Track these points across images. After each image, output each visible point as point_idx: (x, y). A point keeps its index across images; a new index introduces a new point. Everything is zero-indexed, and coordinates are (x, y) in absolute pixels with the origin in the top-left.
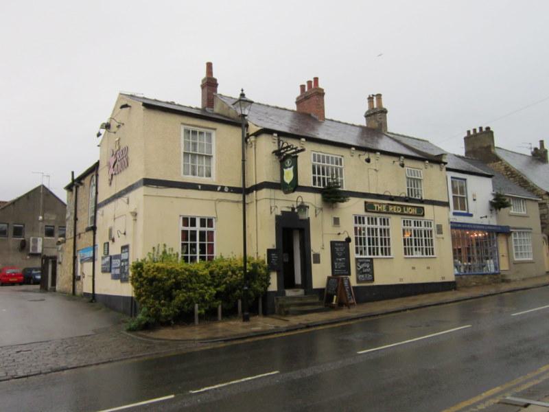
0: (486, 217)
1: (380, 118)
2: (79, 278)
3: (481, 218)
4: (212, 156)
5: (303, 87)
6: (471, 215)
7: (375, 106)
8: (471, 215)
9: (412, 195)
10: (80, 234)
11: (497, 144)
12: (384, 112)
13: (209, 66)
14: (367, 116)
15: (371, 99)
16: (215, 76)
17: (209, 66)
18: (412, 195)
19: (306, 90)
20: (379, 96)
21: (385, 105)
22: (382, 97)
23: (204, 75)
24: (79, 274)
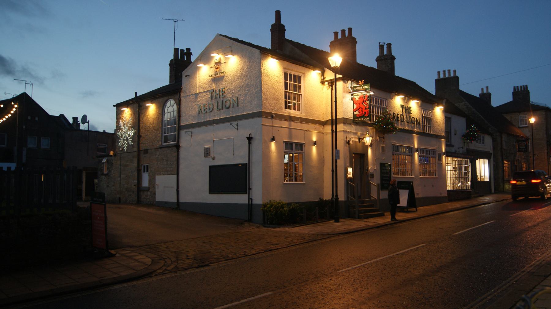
0: (463, 148)
1: (391, 64)
2: (147, 189)
3: (459, 148)
4: (301, 95)
6: (453, 146)
7: (385, 53)
8: (453, 146)
9: (428, 132)
10: (146, 151)
12: (393, 58)
14: (378, 60)
15: (381, 47)
18: (428, 132)
19: (340, 36)
20: (389, 46)
21: (393, 54)
24: (145, 183)
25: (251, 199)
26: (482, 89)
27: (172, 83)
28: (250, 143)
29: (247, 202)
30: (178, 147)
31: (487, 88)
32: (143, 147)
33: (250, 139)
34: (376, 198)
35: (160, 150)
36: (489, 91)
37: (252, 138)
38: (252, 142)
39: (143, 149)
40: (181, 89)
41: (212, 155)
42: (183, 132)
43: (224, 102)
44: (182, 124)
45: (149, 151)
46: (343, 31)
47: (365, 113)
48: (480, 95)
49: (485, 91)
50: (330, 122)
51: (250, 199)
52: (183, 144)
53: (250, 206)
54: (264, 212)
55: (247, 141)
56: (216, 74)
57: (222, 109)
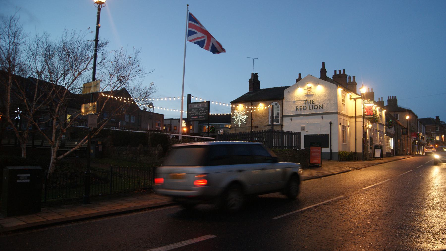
5: (335, 71)
11: (398, 105)
13: (323, 64)
16: (325, 68)
17: (323, 64)
22: (355, 77)
23: (321, 67)
25: (332, 150)
26: (379, 99)
27: (250, 91)
28: (331, 125)
29: (330, 151)
30: (282, 125)
31: (382, 98)
32: (254, 125)
33: (331, 123)
34: (371, 152)
35: (267, 127)
36: (383, 100)
37: (332, 123)
38: (332, 125)
39: (254, 126)
40: (284, 98)
41: (306, 130)
42: (285, 119)
43: (313, 106)
44: (284, 115)
45: (259, 127)
46: (340, 71)
47: (371, 114)
48: (378, 102)
49: (381, 100)
50: (355, 117)
51: (331, 150)
52: (284, 124)
53: (331, 153)
54: (339, 155)
55: (330, 124)
56: (308, 92)
57: (312, 109)
